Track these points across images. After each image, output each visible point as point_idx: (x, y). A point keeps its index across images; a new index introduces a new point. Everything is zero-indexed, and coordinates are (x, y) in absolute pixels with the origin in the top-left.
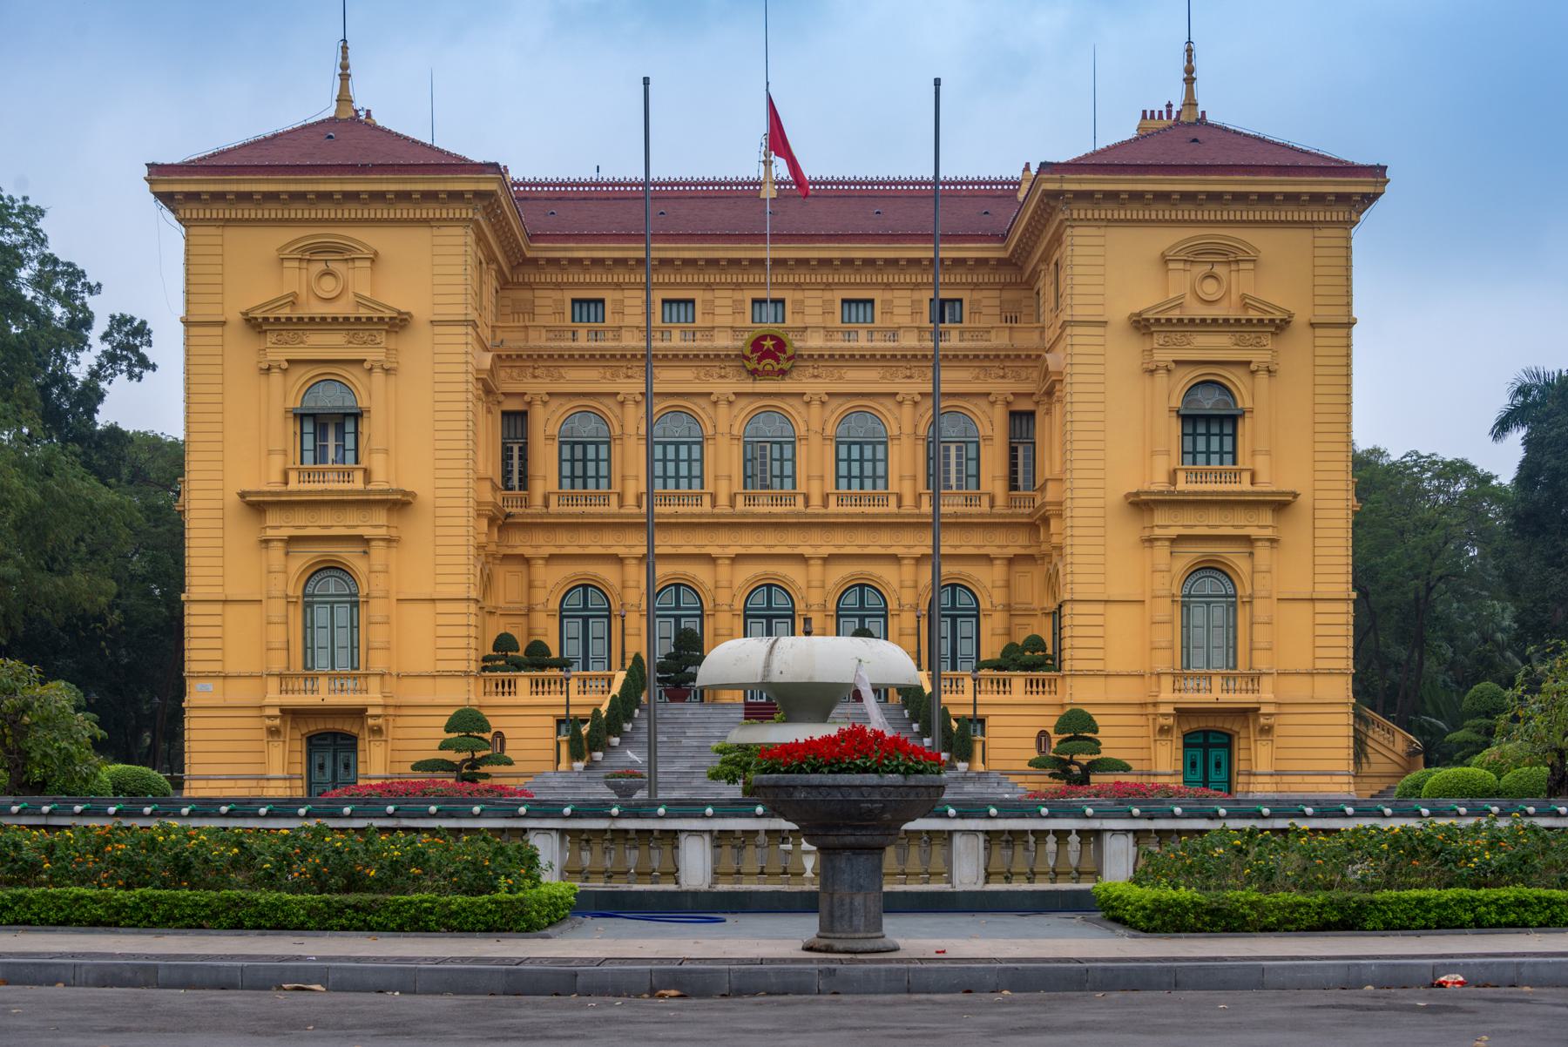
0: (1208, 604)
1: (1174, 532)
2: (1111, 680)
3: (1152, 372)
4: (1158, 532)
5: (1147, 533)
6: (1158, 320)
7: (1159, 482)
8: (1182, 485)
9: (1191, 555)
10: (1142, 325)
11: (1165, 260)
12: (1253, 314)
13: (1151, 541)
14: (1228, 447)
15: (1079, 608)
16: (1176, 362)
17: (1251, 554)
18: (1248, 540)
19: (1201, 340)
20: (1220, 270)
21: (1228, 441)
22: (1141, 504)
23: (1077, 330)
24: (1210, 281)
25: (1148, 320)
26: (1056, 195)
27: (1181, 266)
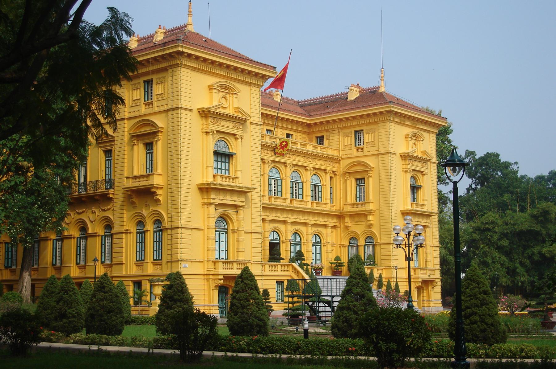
0: (220, 232)
1: (217, 201)
2: (193, 263)
3: (207, 133)
4: (212, 201)
5: (206, 201)
6: (214, 112)
7: (210, 180)
8: (219, 181)
9: (220, 211)
10: (205, 114)
11: (211, 88)
12: (239, 115)
13: (209, 204)
14: (227, 168)
15: (184, 231)
16: (217, 131)
17: (237, 212)
18: (236, 207)
19: (224, 123)
20: (227, 96)
21: (227, 164)
22: (205, 189)
23: (183, 112)
24: (223, 99)
25: (209, 111)
26: (181, 53)
27: (217, 91)
